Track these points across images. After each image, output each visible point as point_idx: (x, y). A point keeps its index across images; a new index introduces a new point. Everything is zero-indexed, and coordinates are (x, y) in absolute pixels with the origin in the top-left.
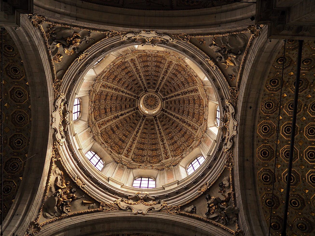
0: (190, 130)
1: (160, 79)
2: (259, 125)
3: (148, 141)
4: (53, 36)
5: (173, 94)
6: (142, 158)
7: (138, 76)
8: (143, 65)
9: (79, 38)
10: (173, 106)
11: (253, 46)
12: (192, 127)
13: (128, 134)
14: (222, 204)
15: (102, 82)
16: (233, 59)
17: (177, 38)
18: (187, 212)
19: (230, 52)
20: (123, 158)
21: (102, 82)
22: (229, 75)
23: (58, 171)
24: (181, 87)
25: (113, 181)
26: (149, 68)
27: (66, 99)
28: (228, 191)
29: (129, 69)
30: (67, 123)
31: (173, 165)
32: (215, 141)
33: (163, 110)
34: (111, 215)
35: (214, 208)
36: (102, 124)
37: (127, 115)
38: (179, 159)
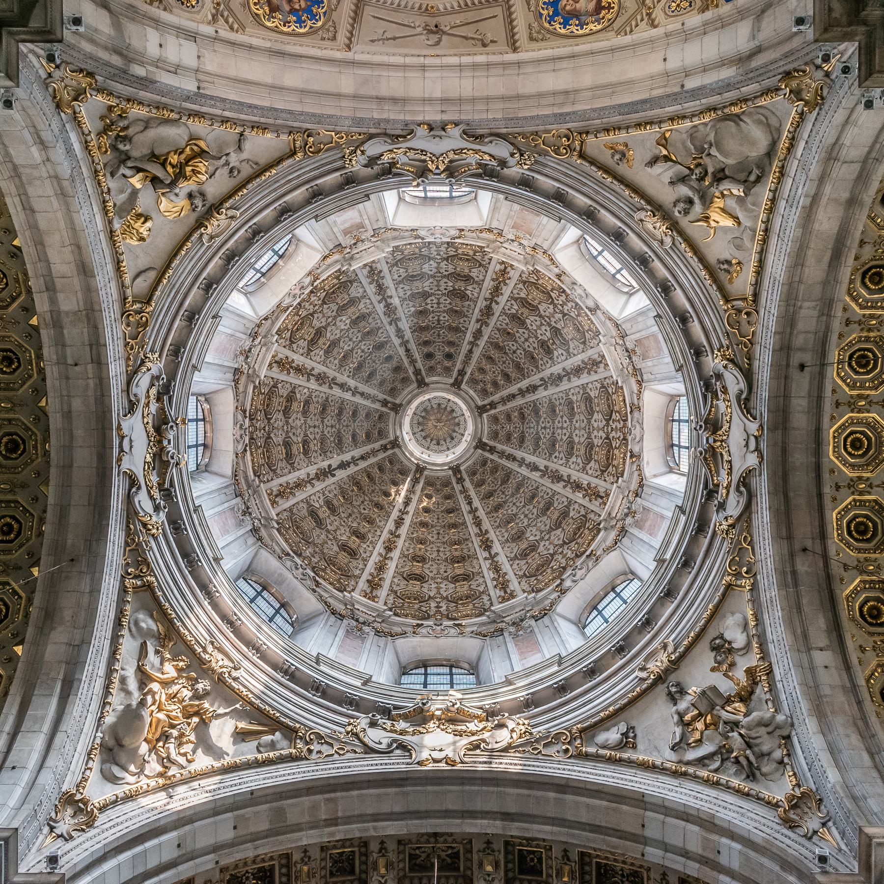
0: (580, 501)
1: (469, 337)
2: (834, 433)
3: (438, 551)
4: (121, 147)
5: (513, 389)
6: (421, 606)
7: (392, 330)
8: (409, 293)
9: (207, 155)
10: (516, 427)
11: (802, 144)
12: (585, 490)
13: (369, 531)
14: (728, 708)
15: (276, 349)
16: (731, 203)
17: (536, 145)
18: (604, 747)
19: (720, 176)
20: (358, 602)
21: (276, 349)
22: (720, 262)
23: (146, 622)
24: (542, 359)
25: (332, 665)
26: (428, 301)
27: (164, 376)
28: (744, 663)
29: (361, 306)
30: (172, 461)
31: (533, 617)
32: (681, 509)
33: (480, 445)
34: (338, 768)
35: (700, 725)
36: (280, 494)
37: (363, 465)
38: (552, 597)
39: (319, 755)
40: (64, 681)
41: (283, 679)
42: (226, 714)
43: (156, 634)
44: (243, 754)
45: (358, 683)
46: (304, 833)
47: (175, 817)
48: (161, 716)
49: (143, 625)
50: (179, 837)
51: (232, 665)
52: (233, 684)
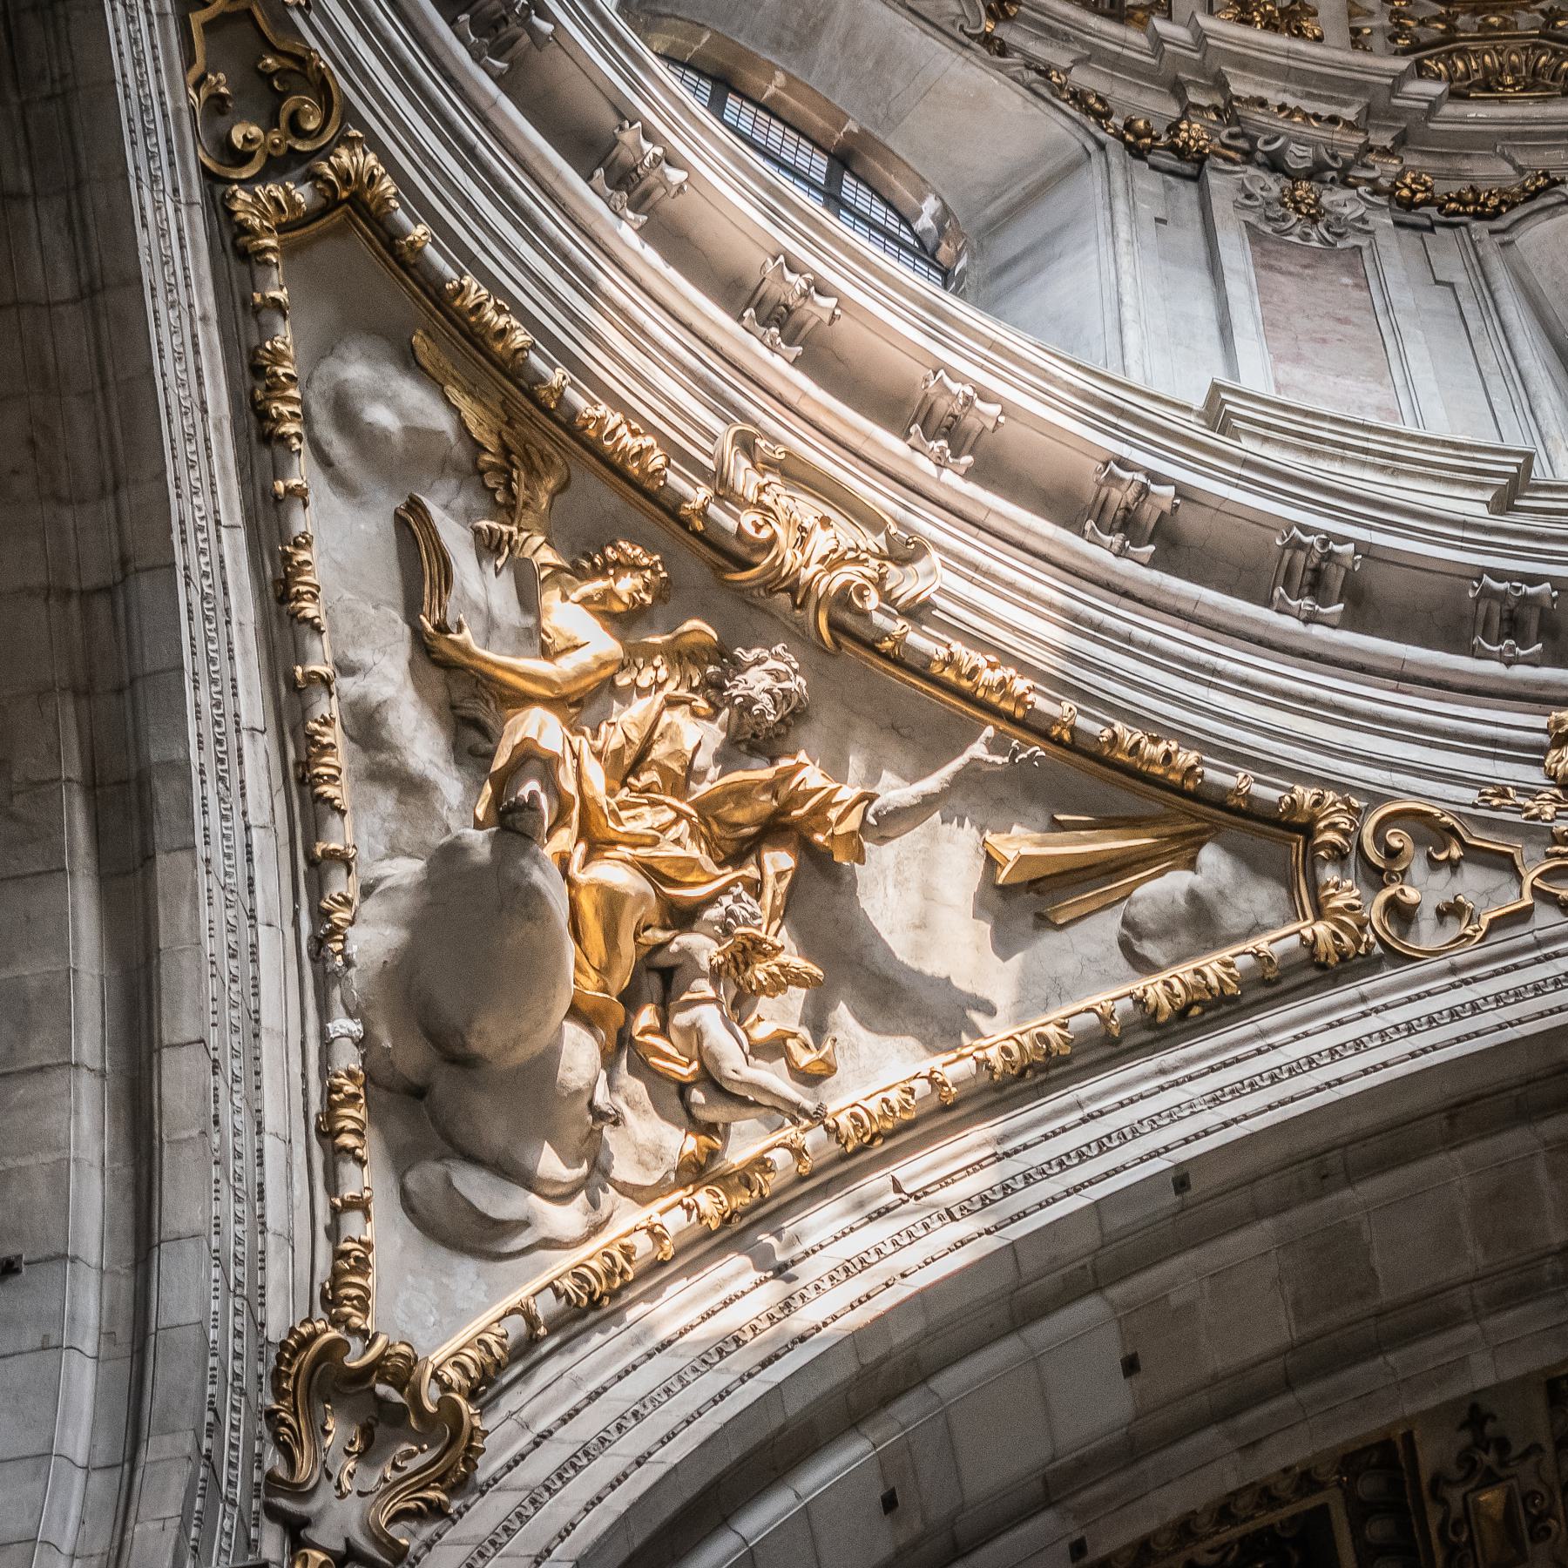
20: (1244, 63)
23: (391, 401)
39: (1454, 929)
40: (93, 786)
41: (1125, 566)
42: (928, 803)
43: (459, 451)
44: (1061, 992)
45: (1473, 505)
46: (1470, 1330)
47: (844, 1370)
48: (614, 873)
49: (380, 416)
50: (882, 1460)
51: (874, 542)
52: (914, 639)
